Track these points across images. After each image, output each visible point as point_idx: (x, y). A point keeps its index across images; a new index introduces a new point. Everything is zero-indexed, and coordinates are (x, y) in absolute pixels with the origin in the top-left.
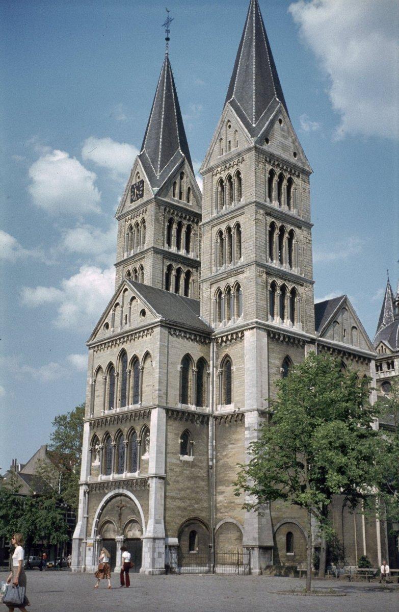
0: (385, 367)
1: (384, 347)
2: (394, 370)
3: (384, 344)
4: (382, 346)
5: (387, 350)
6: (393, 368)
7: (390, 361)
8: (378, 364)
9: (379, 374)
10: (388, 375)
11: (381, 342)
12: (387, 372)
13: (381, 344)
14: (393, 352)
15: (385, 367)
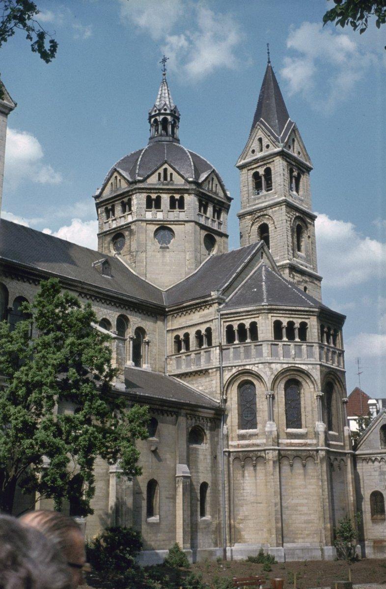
0: (118, 209)
1: (119, 178)
2: (131, 214)
3: (118, 172)
4: (116, 177)
5: (122, 181)
6: (130, 210)
7: (126, 200)
8: (110, 207)
9: (110, 222)
10: (122, 222)
11: (115, 170)
12: (120, 217)
13: (116, 174)
14: (130, 183)
15: (118, 209)
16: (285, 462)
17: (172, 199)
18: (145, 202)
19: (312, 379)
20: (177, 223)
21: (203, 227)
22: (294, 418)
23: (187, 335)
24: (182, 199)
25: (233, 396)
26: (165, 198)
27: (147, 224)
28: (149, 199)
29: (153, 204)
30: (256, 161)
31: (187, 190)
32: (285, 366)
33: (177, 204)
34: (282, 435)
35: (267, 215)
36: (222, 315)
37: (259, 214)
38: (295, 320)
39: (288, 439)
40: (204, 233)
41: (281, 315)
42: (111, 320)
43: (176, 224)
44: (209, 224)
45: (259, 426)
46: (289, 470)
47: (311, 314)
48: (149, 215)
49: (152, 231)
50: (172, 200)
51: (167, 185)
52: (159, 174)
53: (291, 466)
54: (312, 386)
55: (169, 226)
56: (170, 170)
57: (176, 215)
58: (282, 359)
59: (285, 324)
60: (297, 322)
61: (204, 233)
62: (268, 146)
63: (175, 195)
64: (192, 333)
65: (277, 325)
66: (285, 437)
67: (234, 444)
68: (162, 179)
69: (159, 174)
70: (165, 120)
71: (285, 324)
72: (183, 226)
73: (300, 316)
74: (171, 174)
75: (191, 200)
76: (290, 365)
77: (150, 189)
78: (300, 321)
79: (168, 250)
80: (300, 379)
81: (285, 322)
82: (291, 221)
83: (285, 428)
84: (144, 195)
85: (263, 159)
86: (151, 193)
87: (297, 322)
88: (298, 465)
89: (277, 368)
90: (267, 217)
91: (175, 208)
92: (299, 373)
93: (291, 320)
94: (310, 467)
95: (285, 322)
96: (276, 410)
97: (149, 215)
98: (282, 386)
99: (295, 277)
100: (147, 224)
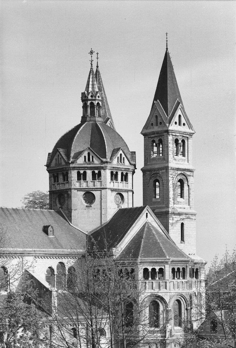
2: (68, 183)
9: (56, 185)
12: (62, 184)
18: (77, 176)
20: (96, 190)
26: (89, 173)
27: (78, 191)
30: (153, 133)
31: (102, 167)
33: (97, 176)
35: (158, 174)
37: (154, 172)
40: (114, 193)
41: (148, 265)
43: (96, 191)
47: (166, 263)
49: (81, 196)
50: (93, 173)
51: (90, 164)
52: (85, 157)
55: (92, 192)
57: (98, 185)
60: (157, 268)
61: (114, 193)
62: (161, 123)
65: (146, 270)
68: (87, 160)
69: (85, 157)
71: (150, 270)
73: (159, 265)
79: (91, 208)
81: (150, 269)
82: (173, 180)
84: (76, 171)
85: (158, 133)
86: (80, 170)
87: (157, 268)
90: (159, 175)
91: (96, 180)
93: (154, 267)
95: (150, 269)
99: (174, 219)
100: (78, 191)
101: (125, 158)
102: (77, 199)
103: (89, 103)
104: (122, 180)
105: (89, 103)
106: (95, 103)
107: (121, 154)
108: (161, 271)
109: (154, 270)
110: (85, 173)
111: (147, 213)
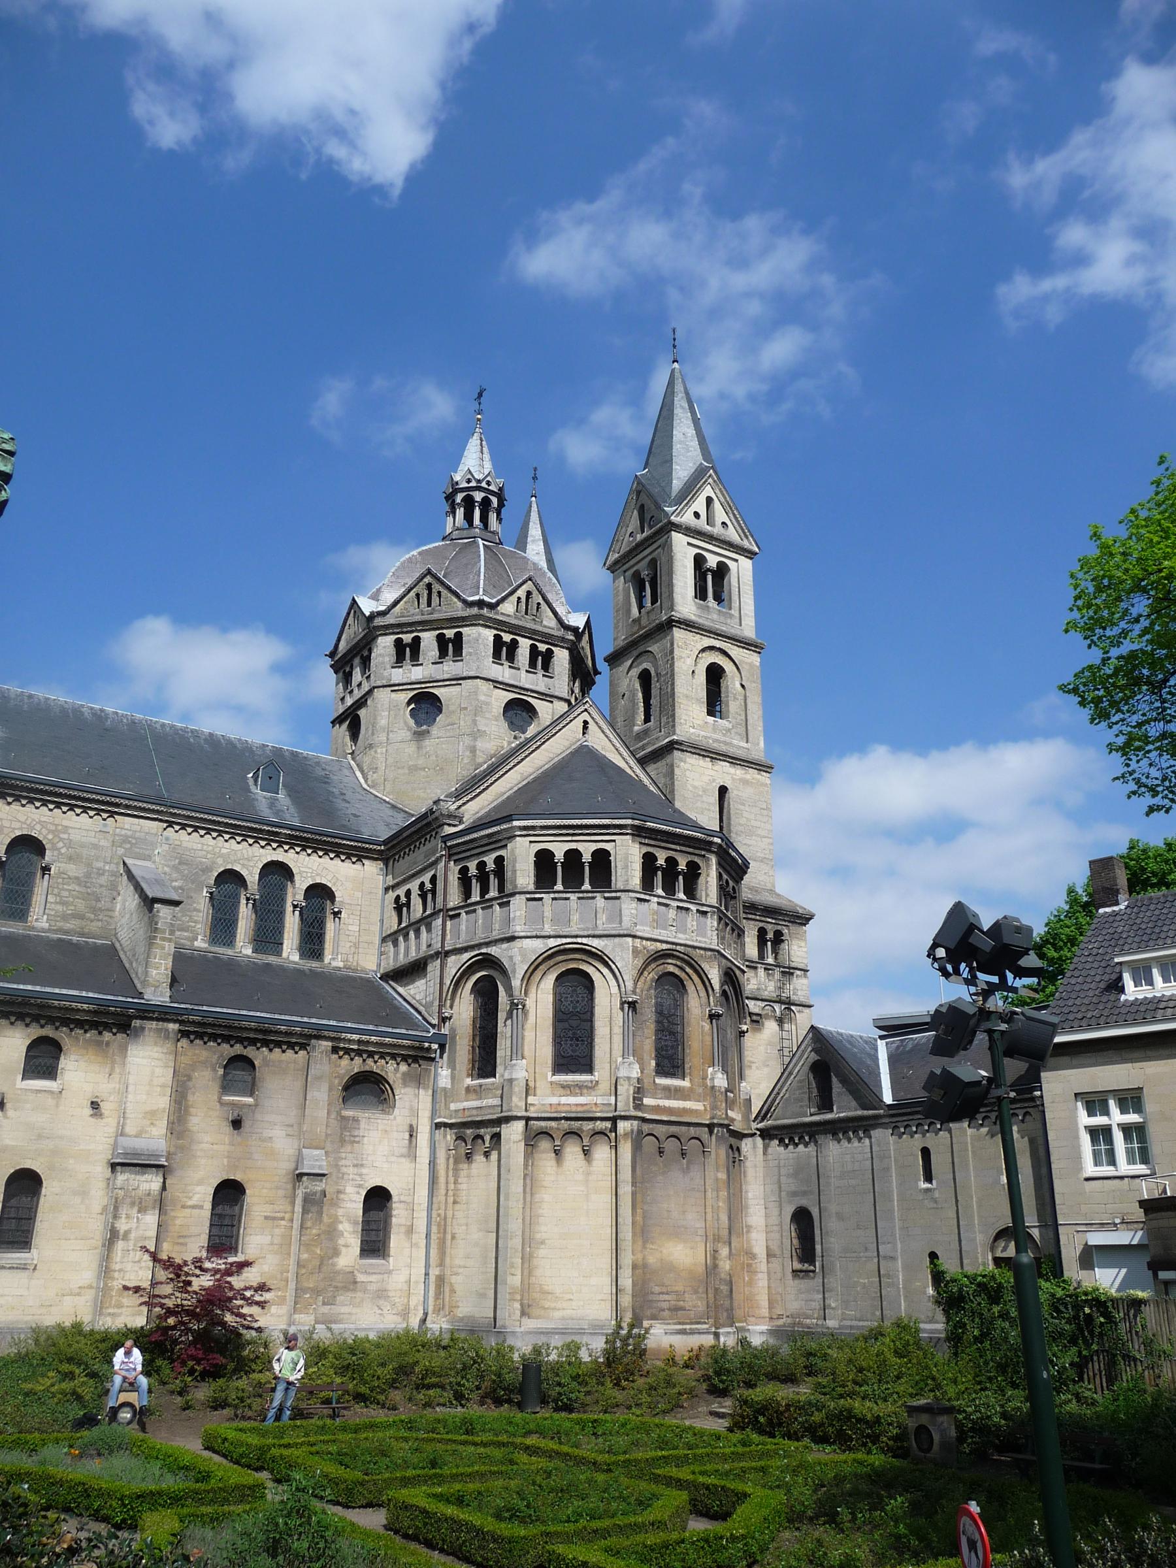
16: (545, 1144)
17: (441, 639)
19: (613, 967)
21: (497, 684)
22: (574, 1050)
23: (408, 894)
24: (459, 636)
25: (464, 1009)
26: (428, 639)
28: (399, 645)
29: (407, 652)
32: (552, 943)
33: (451, 647)
34: (542, 1087)
36: (450, 848)
38: (580, 847)
39: (554, 1095)
42: (244, 873)
44: (525, 679)
45: (499, 1069)
46: (553, 1163)
48: (398, 675)
52: (418, 595)
53: (557, 1153)
54: (613, 982)
56: (436, 587)
57: (450, 668)
58: (548, 929)
59: (559, 856)
60: (587, 851)
63: (444, 631)
64: (414, 886)
65: (544, 860)
66: (548, 1091)
67: (463, 1107)
70: (469, 503)
71: (559, 856)
72: (458, 688)
74: (439, 593)
75: (480, 638)
76: (564, 941)
77: (399, 625)
78: (594, 847)
80: (590, 970)
81: (559, 850)
83: (550, 1074)
87: (587, 851)
88: (572, 1151)
89: (537, 947)
92: (584, 957)
93: (573, 846)
94: (602, 1152)
95: (559, 850)
96: (529, 1035)
97: (398, 675)
98: (549, 982)
101: (544, 606)
102: (388, 712)
103: (459, 498)
104: (533, 664)
105: (459, 498)
106: (478, 496)
107: (529, 594)
108: (602, 860)
109: (573, 856)
110: (417, 640)
111: (586, 723)
